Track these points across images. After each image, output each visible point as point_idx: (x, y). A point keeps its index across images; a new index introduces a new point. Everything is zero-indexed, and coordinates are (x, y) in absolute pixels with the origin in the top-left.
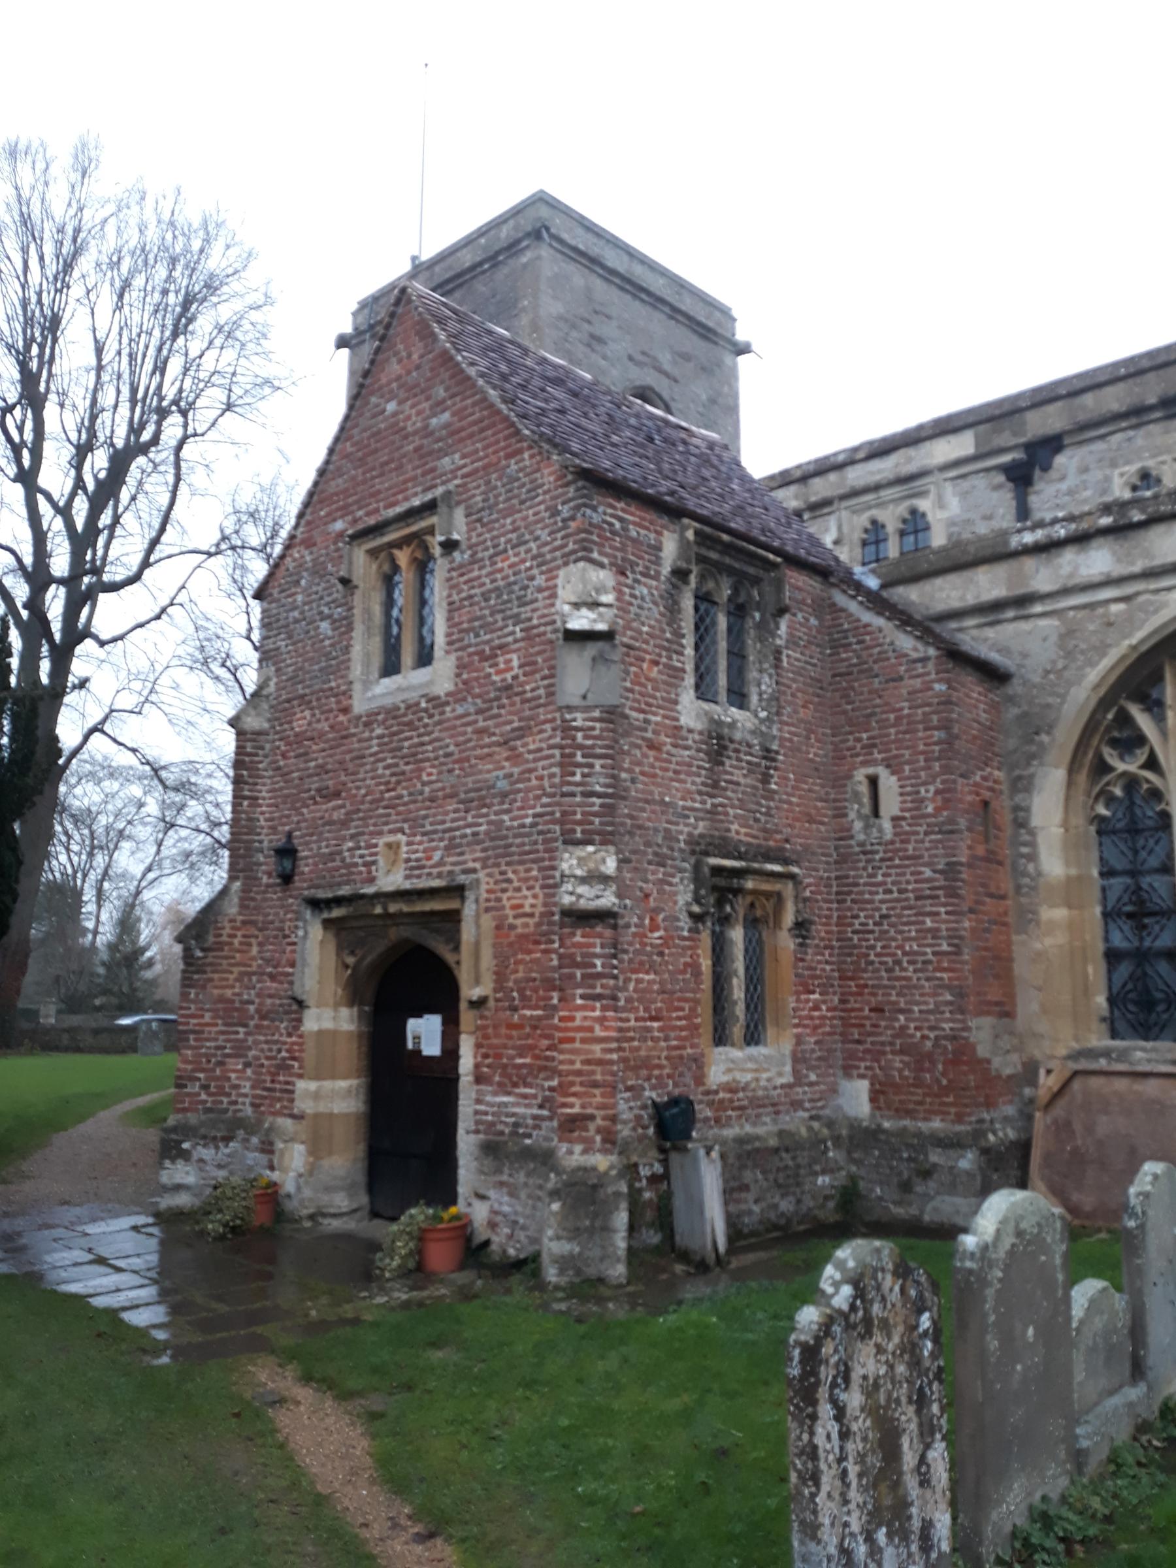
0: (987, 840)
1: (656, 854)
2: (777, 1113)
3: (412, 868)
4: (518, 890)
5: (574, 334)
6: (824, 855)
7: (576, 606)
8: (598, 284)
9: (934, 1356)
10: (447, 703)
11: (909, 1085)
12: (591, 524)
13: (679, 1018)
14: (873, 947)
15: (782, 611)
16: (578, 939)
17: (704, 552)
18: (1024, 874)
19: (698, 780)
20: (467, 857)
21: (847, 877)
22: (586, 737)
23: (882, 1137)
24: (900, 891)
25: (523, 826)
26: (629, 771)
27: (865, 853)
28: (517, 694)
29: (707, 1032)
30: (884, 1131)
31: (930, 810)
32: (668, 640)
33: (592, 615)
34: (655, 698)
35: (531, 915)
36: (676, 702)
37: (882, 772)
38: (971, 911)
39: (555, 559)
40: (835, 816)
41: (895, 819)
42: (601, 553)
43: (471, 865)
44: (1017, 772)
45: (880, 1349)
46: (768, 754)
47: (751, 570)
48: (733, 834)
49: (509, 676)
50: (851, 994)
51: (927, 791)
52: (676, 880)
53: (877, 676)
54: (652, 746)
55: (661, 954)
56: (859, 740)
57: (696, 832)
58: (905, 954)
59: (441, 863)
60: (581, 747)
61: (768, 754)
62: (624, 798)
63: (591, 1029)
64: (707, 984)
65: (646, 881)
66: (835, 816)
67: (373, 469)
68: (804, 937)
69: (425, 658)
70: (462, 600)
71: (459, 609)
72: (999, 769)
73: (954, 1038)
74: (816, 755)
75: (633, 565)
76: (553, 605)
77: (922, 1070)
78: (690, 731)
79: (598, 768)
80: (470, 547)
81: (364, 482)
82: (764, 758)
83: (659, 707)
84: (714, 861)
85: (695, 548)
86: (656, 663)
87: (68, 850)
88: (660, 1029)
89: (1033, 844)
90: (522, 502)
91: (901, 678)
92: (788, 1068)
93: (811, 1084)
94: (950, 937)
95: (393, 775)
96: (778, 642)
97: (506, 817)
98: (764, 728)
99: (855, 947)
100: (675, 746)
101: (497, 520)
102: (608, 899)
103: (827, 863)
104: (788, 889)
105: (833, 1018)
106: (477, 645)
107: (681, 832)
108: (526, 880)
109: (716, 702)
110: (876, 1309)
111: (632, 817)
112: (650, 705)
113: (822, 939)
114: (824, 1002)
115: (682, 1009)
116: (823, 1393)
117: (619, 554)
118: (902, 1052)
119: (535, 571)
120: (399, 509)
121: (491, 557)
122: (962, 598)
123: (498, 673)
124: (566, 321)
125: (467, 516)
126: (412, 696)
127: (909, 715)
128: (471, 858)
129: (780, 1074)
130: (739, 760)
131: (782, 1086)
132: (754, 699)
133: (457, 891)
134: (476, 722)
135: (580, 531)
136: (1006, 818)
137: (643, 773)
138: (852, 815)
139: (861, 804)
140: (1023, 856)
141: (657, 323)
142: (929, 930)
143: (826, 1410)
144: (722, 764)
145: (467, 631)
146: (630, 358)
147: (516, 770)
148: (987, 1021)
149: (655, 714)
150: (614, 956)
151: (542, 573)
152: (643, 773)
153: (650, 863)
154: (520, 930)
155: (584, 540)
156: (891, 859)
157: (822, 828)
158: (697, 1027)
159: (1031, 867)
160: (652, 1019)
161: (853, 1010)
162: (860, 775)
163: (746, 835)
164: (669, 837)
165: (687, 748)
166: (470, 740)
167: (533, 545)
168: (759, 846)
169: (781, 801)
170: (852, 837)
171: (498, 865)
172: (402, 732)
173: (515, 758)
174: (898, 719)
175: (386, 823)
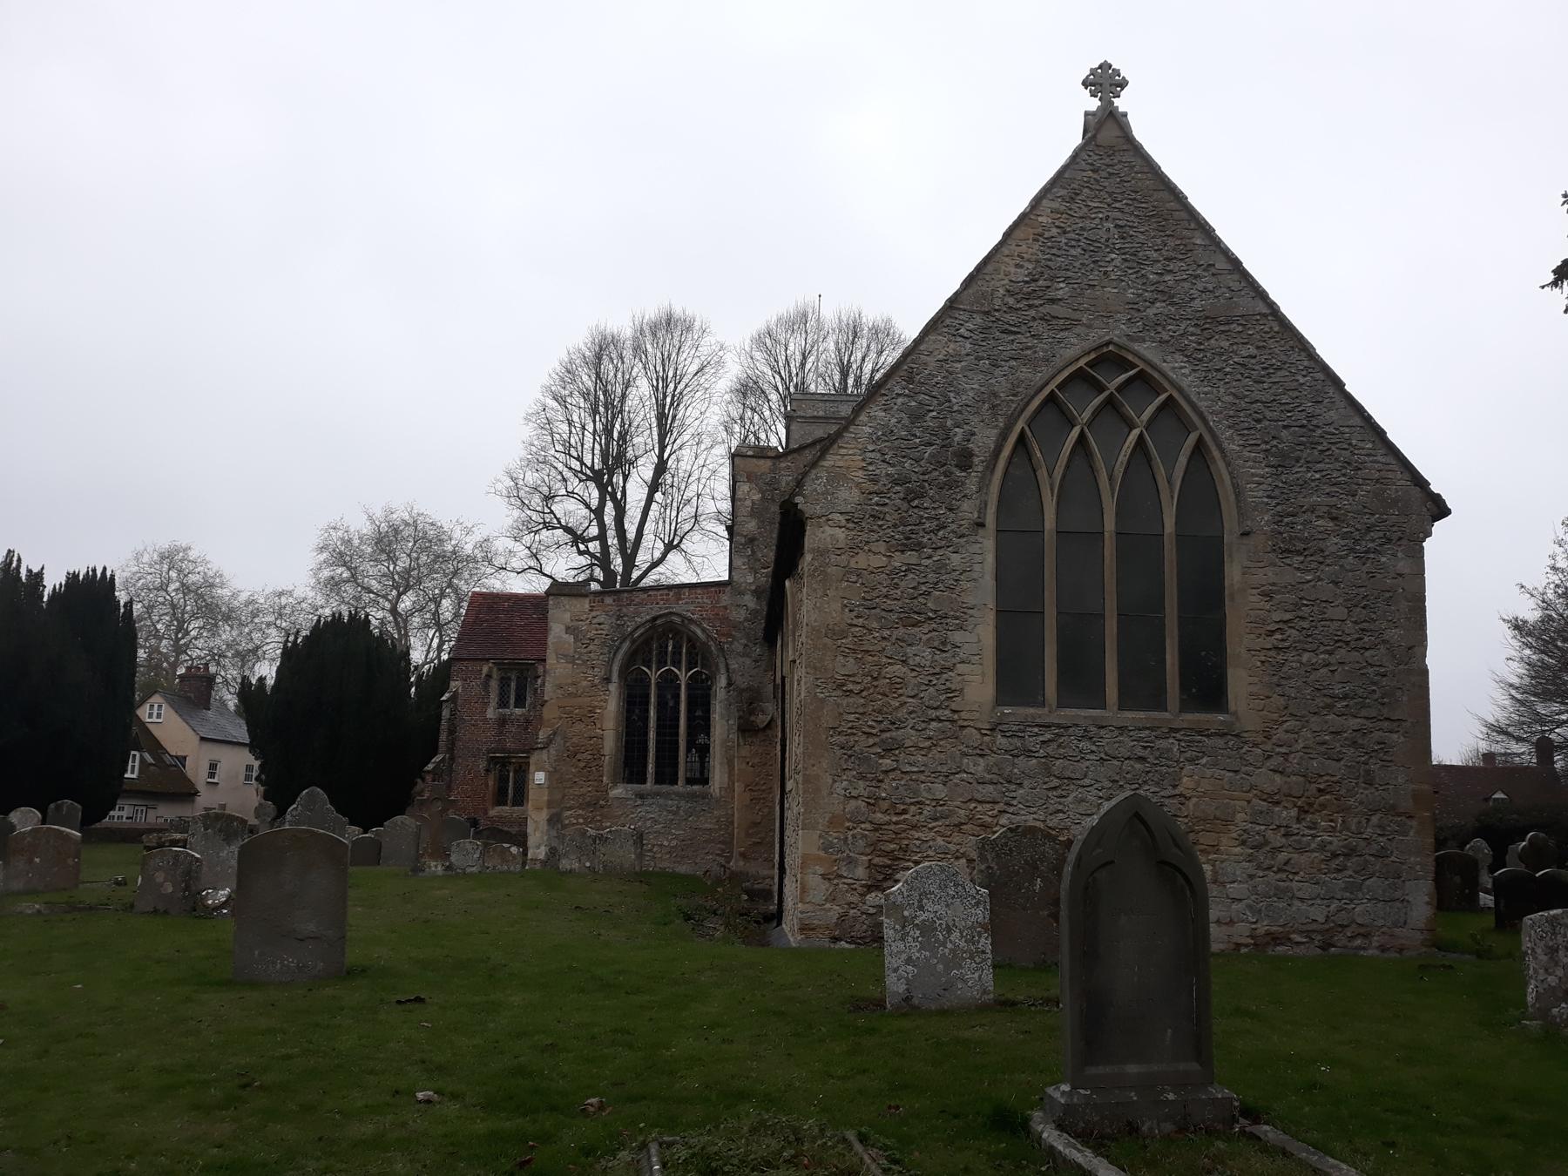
15: (539, 677)
61: (528, 721)
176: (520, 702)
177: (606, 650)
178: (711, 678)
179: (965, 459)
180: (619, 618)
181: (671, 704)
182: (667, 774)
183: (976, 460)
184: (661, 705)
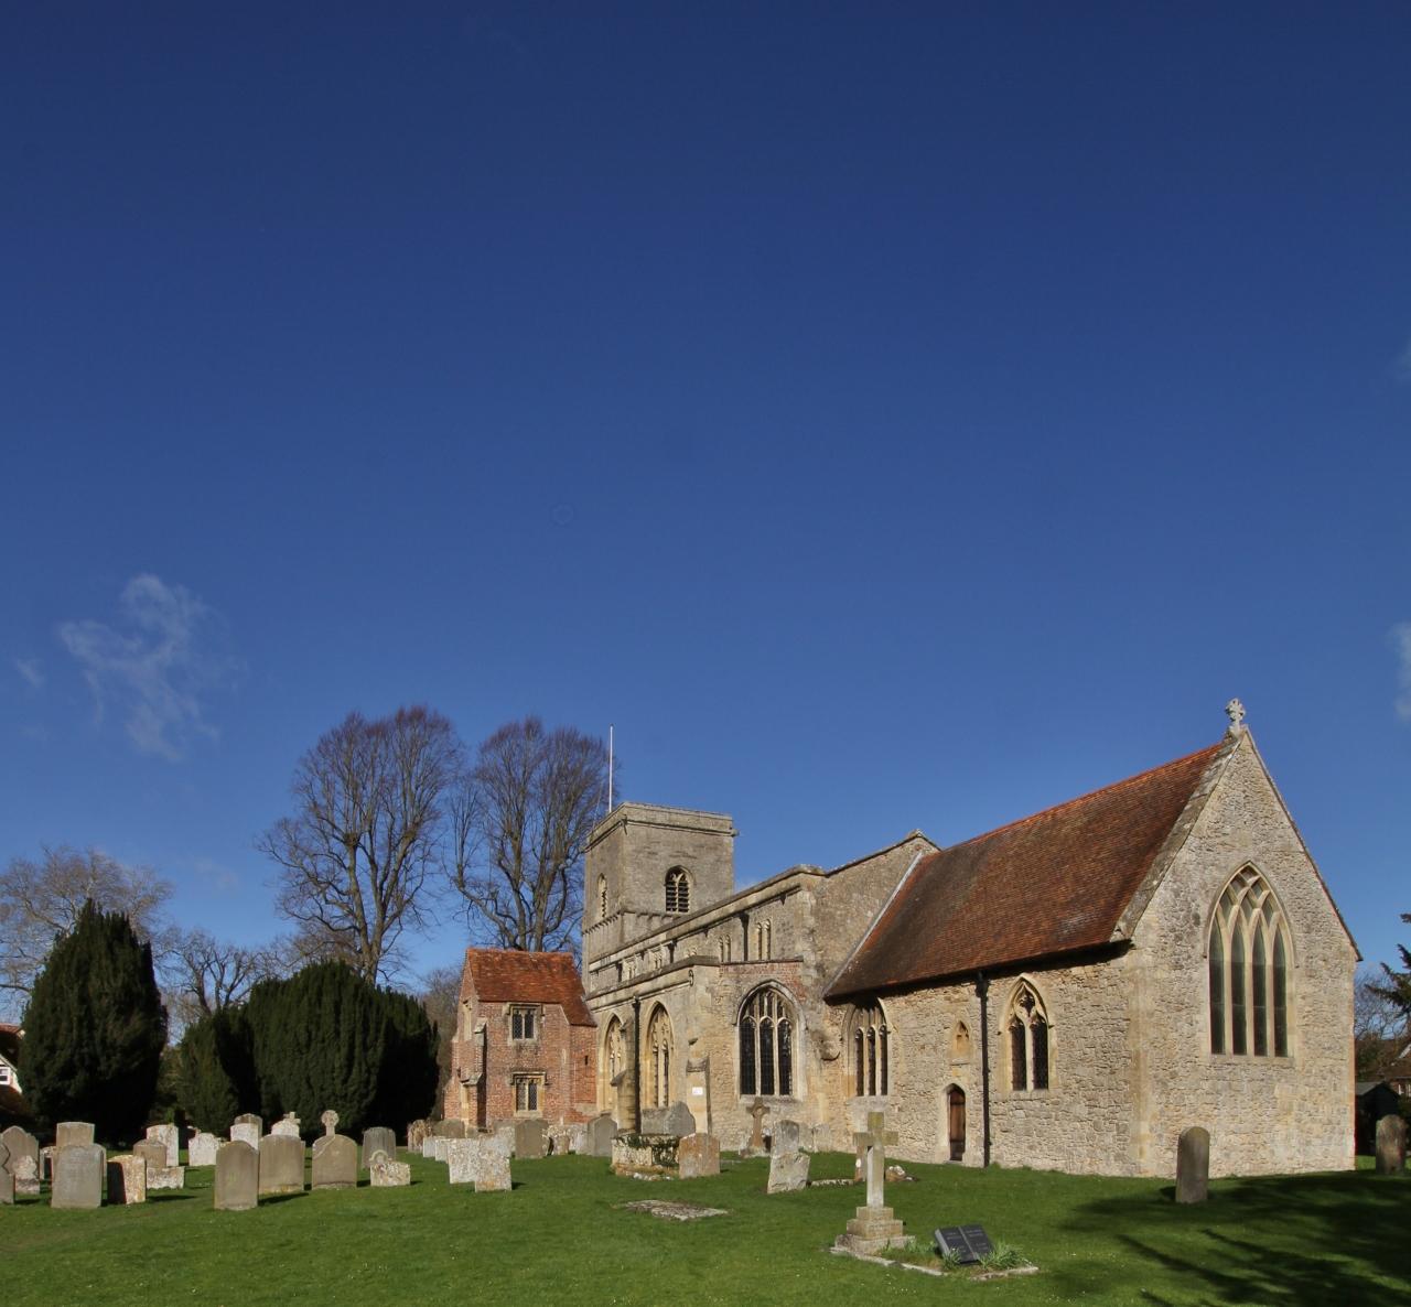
0: (586, 1063)
5: (641, 855)
8: (653, 831)
46: (537, 1047)
61: (537, 1047)
141: (686, 836)
146: (671, 856)
176: (529, 1034)
177: (731, 1004)
178: (792, 1024)
179: (1197, 917)
180: (738, 982)
181: (768, 1041)
182: (768, 1089)
183: (1201, 920)
184: (763, 1042)
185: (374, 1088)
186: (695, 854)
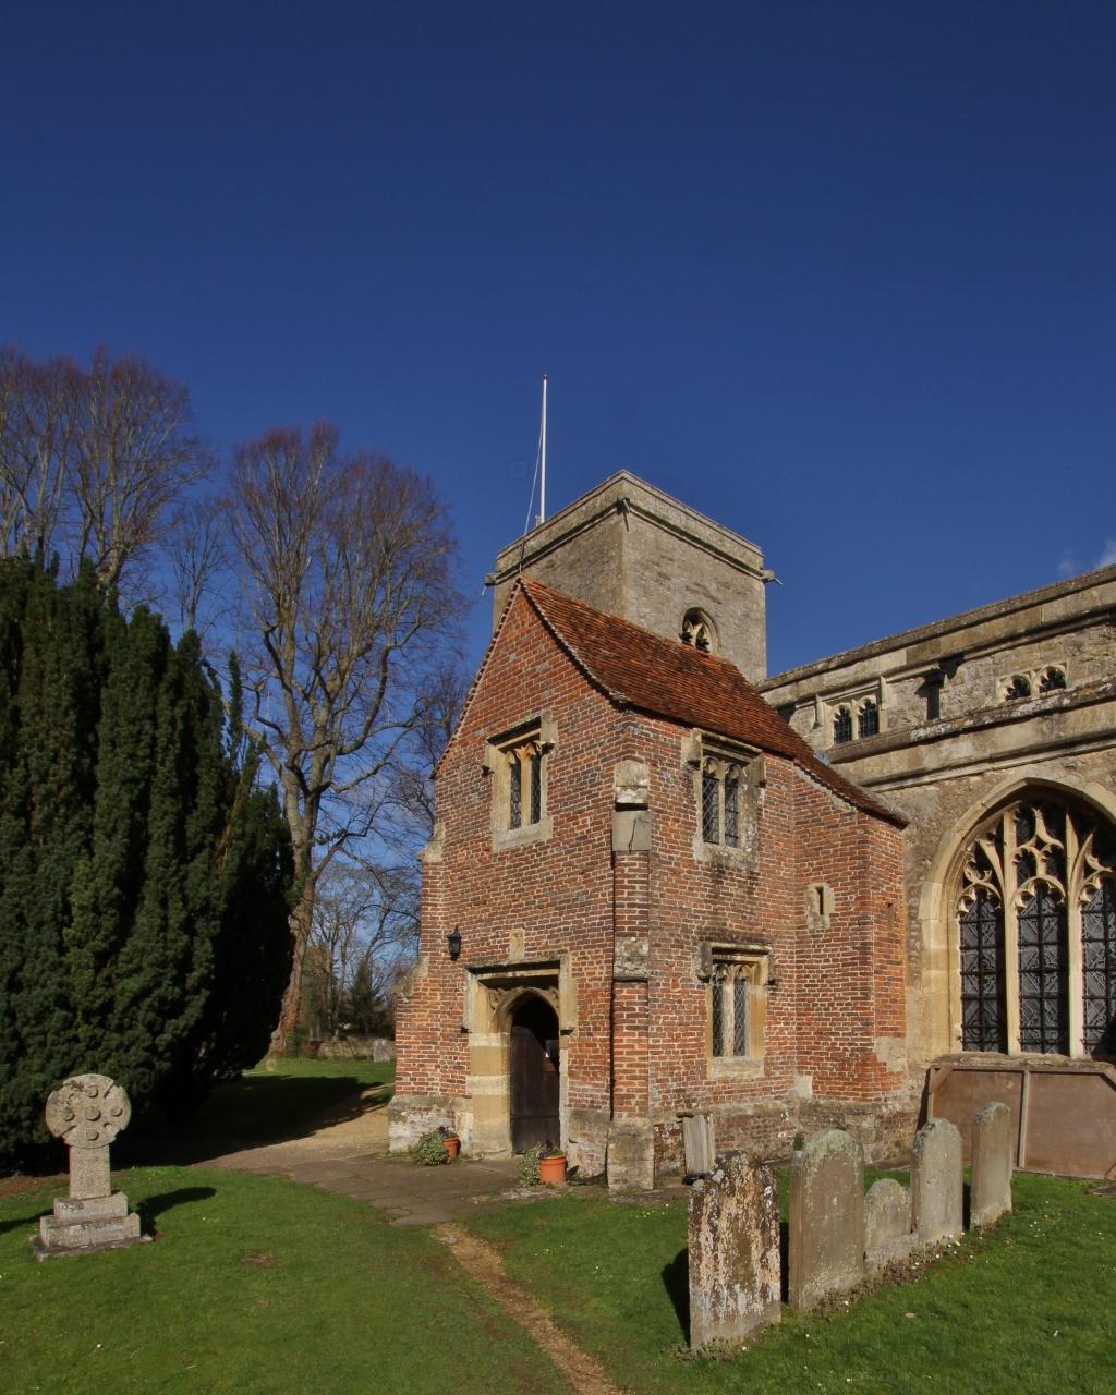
1: (677, 941)
2: (755, 1095)
3: (529, 950)
4: (592, 963)
5: (647, 574)
6: (789, 938)
7: (624, 787)
9: (772, 1207)
10: (549, 847)
11: (836, 1079)
12: (633, 736)
13: (690, 1040)
14: (817, 995)
16: (624, 994)
17: (709, 748)
18: (914, 949)
19: (706, 894)
20: (562, 943)
21: (803, 952)
22: (630, 870)
23: (819, 1109)
24: (834, 961)
25: (594, 924)
26: (659, 889)
27: (814, 937)
28: (591, 842)
29: (709, 1047)
30: (820, 1106)
31: (852, 910)
32: (685, 806)
33: (634, 794)
34: (676, 843)
35: (600, 979)
36: (691, 845)
37: (825, 886)
38: (876, 972)
39: (611, 757)
40: (796, 914)
41: (831, 915)
42: (639, 753)
43: (563, 948)
44: (911, 884)
45: (738, 1202)
46: (752, 876)
47: (741, 758)
48: (728, 927)
49: (585, 830)
50: (804, 1024)
51: (851, 898)
52: (690, 956)
53: (823, 824)
54: (674, 873)
55: (680, 1002)
56: (811, 865)
57: (703, 927)
58: (835, 999)
59: (546, 947)
60: (627, 876)
61: (752, 876)
62: (657, 907)
63: (633, 1047)
64: (709, 1020)
65: (670, 957)
66: (796, 914)
67: (502, 696)
68: (774, 990)
69: (536, 817)
70: (557, 781)
71: (554, 787)
72: (900, 883)
73: (863, 1050)
74: (784, 874)
75: (662, 759)
76: (610, 786)
77: (843, 1069)
78: (700, 863)
79: (638, 890)
80: (560, 748)
81: (497, 704)
82: (750, 878)
83: (679, 848)
84: (714, 944)
85: (703, 746)
86: (678, 821)
87: (321, 925)
88: (679, 1046)
89: (920, 930)
90: (592, 721)
91: (837, 826)
92: (762, 1069)
93: (778, 1078)
94: (862, 989)
95: (516, 891)
96: (759, 803)
97: (584, 919)
98: (749, 859)
99: (806, 995)
100: (690, 872)
101: (577, 732)
102: (642, 971)
103: (792, 943)
104: (764, 960)
105: (793, 1038)
106: (566, 810)
107: (693, 927)
108: (596, 957)
109: (718, 844)
110: (737, 1183)
111: (662, 918)
112: (674, 848)
113: (786, 990)
114: (787, 1029)
115: (693, 1034)
116: (704, 1219)
117: (652, 753)
118: (832, 1059)
119: (600, 765)
120: (518, 723)
121: (573, 755)
122: (881, 771)
123: (579, 828)
124: (642, 565)
125: (559, 728)
126: (528, 842)
127: (841, 850)
128: (564, 943)
129: (756, 1073)
130: (732, 880)
131: (757, 1079)
132: (744, 840)
133: (556, 964)
134: (565, 858)
135: (626, 740)
136: (903, 913)
137: (668, 891)
138: (807, 913)
139: (812, 906)
140: (912, 937)
142: (850, 985)
143: (705, 1227)
144: (722, 883)
145: (560, 801)
146: (687, 589)
147: (590, 890)
148: (885, 1040)
149: (676, 853)
150: (647, 1004)
151: (604, 766)
152: (668, 891)
153: (673, 946)
154: (593, 988)
155: (628, 746)
156: (829, 941)
157: (788, 921)
158: (702, 1045)
159: (918, 945)
160: (673, 1040)
161: (804, 1034)
162: (812, 887)
163: (737, 927)
164: (686, 930)
165: (697, 873)
166: (562, 870)
167: (598, 748)
168: (745, 933)
169: (760, 905)
170: (806, 927)
171: (580, 948)
172: (522, 864)
173: (588, 882)
174: (835, 851)
175: (513, 922)
185: (204, 981)
186: (720, 596)
